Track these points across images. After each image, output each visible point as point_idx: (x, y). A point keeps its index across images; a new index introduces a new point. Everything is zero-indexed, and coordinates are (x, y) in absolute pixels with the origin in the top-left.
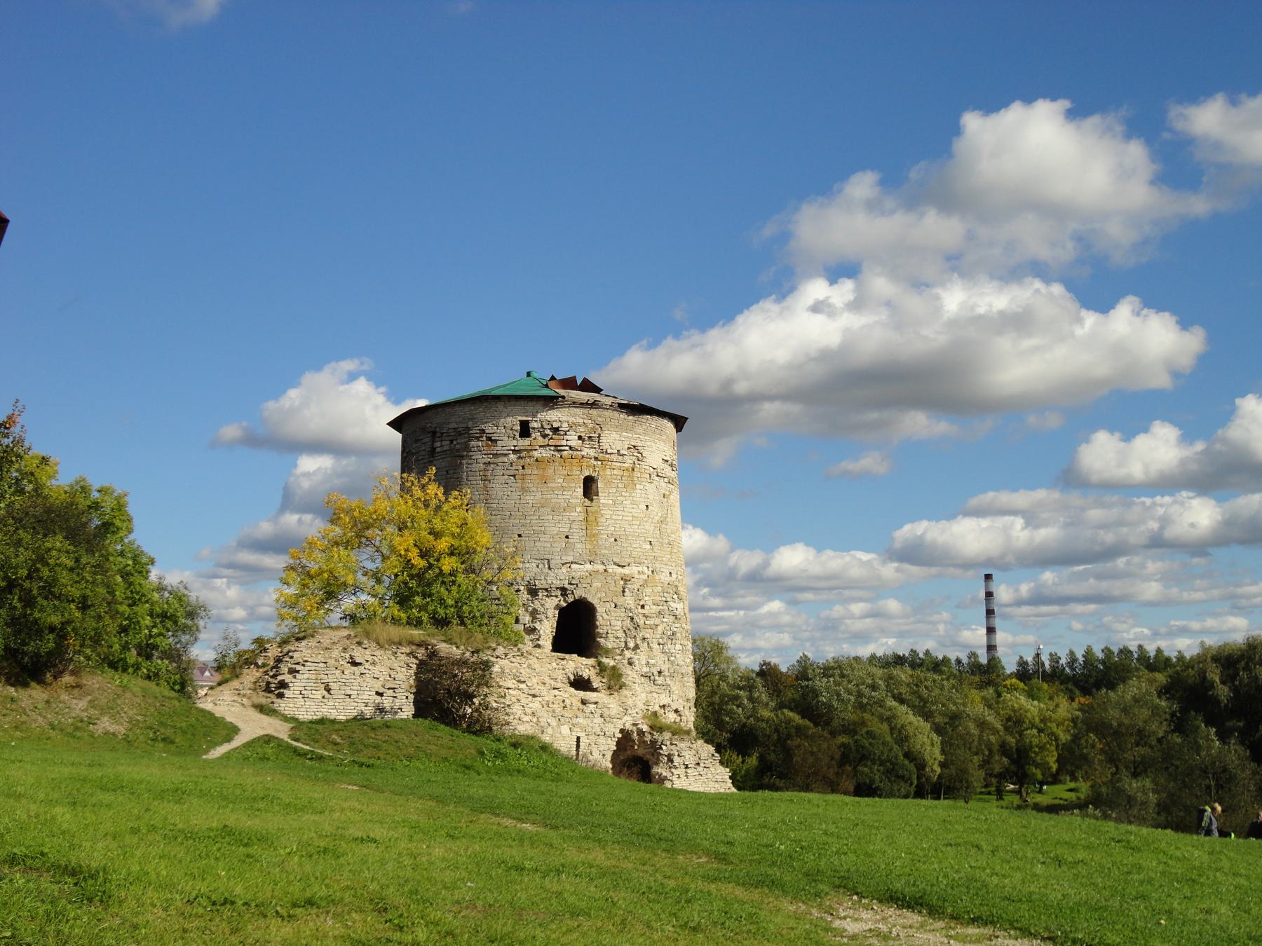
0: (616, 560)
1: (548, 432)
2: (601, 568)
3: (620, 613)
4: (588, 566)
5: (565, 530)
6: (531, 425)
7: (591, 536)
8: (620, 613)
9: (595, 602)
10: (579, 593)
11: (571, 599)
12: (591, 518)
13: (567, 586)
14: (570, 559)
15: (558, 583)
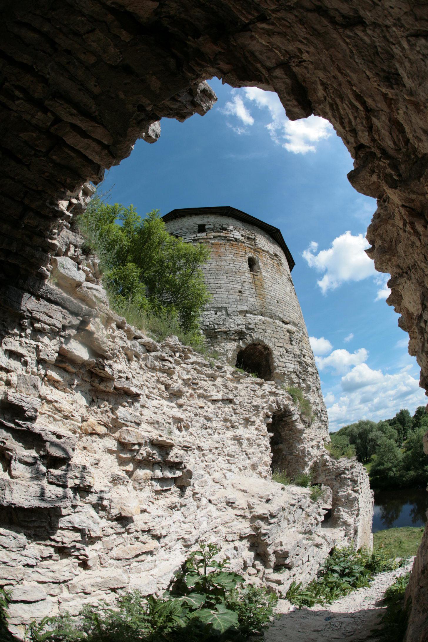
0: (281, 316)
1: (219, 230)
2: (270, 320)
3: (290, 357)
4: (260, 317)
5: (239, 287)
6: (207, 227)
7: (260, 295)
8: (290, 357)
9: (271, 345)
10: (255, 336)
11: (249, 340)
12: (257, 283)
13: (244, 330)
14: (245, 308)
15: (238, 328)
